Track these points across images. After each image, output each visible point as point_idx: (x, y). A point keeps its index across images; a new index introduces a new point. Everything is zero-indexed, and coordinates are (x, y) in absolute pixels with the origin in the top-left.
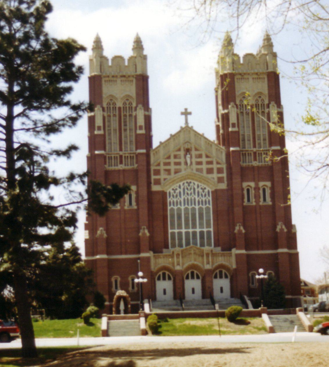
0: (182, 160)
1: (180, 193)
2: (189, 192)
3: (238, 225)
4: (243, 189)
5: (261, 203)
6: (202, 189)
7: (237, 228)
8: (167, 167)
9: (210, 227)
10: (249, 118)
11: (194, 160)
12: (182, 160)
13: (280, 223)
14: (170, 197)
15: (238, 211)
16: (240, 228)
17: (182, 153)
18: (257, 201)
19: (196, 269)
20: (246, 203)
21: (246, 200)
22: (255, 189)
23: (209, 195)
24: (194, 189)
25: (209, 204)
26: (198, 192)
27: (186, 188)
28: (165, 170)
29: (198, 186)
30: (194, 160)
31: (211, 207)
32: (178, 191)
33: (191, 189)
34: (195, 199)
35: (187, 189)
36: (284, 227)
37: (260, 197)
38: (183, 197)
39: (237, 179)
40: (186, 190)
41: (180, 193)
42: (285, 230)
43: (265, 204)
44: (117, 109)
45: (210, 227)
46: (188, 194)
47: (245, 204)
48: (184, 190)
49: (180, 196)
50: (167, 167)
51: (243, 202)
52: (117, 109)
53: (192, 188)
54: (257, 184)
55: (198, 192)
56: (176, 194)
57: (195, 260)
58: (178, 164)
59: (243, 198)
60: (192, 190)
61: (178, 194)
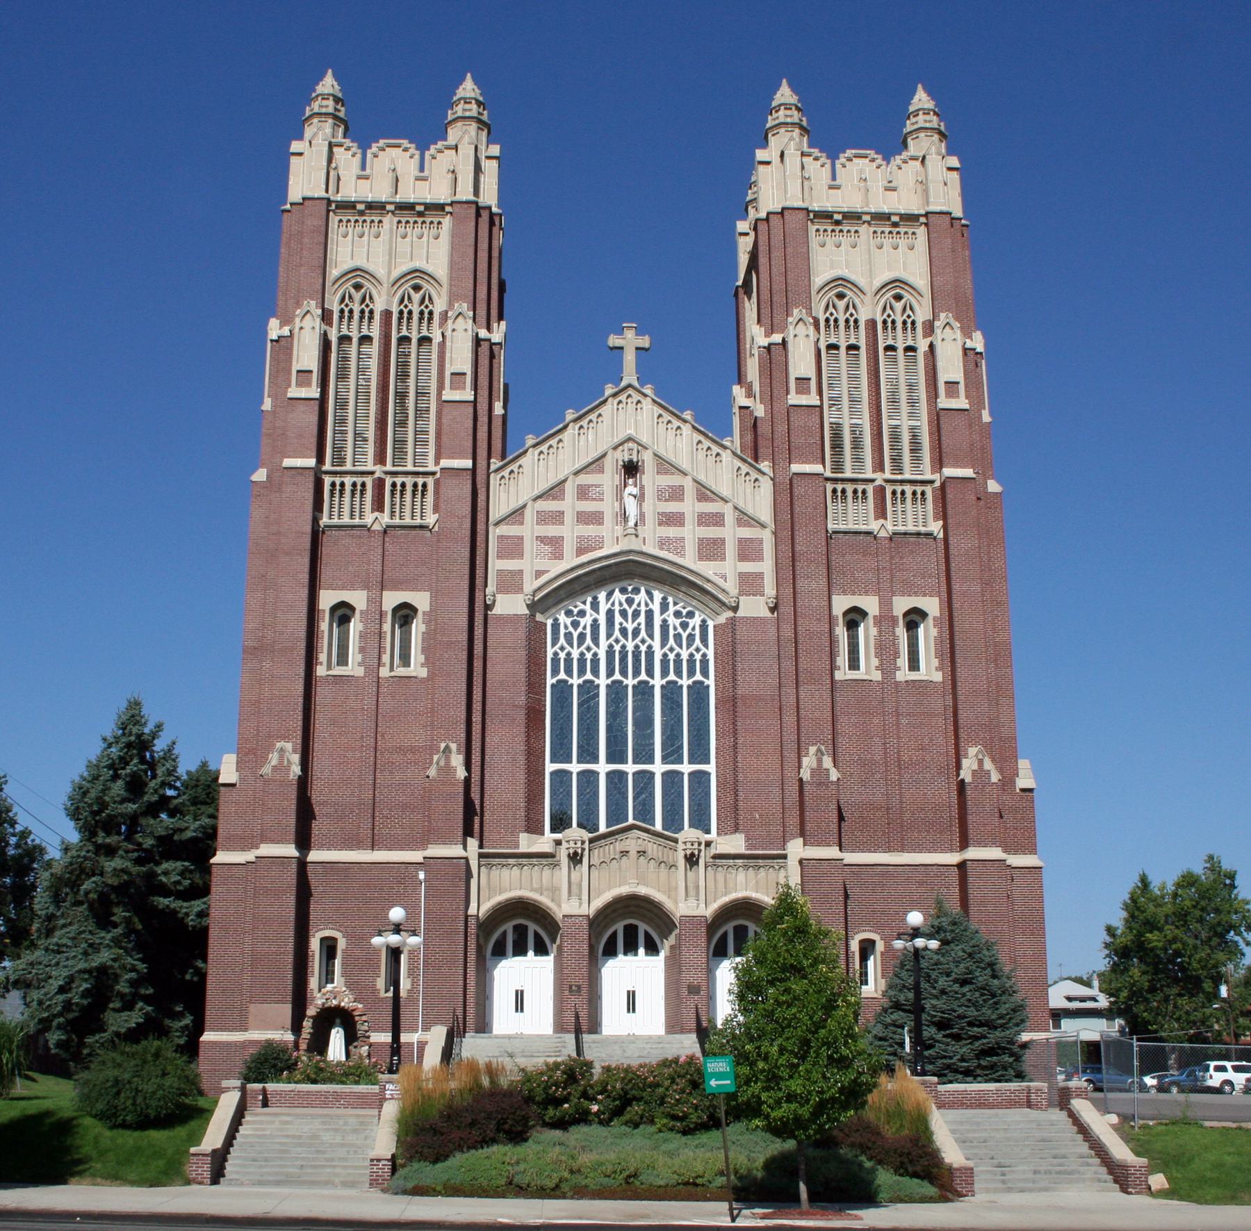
0: (608, 507)
1: (595, 625)
2: (630, 627)
3: (812, 750)
4: (831, 620)
5: (904, 674)
6: (677, 614)
7: (808, 762)
8: (551, 531)
9: (706, 761)
10: (857, 366)
11: (652, 506)
12: (608, 507)
13: (972, 751)
14: (555, 641)
15: (815, 700)
16: (820, 761)
17: (609, 478)
18: (888, 666)
19: (643, 918)
20: (843, 673)
21: (843, 659)
22: (878, 621)
23: (704, 640)
24: (650, 614)
25: (705, 673)
26: (665, 626)
27: (617, 608)
28: (542, 540)
29: (664, 607)
30: (652, 506)
31: (711, 682)
32: (587, 621)
33: (636, 614)
34: (650, 653)
35: (624, 613)
36: (988, 765)
37: (896, 655)
38: (604, 643)
39: (812, 584)
40: (618, 619)
41: (595, 625)
42: (995, 777)
43: (914, 676)
44: (377, 317)
45: (706, 761)
46: (624, 631)
47: (839, 676)
48: (610, 614)
49: (596, 640)
50: (551, 531)
51: (833, 668)
52: (377, 317)
53: (643, 608)
54: (886, 604)
55: (665, 626)
56: (580, 629)
57: (642, 881)
58: (595, 518)
59: (832, 656)
60: (642, 619)
61: (588, 631)
